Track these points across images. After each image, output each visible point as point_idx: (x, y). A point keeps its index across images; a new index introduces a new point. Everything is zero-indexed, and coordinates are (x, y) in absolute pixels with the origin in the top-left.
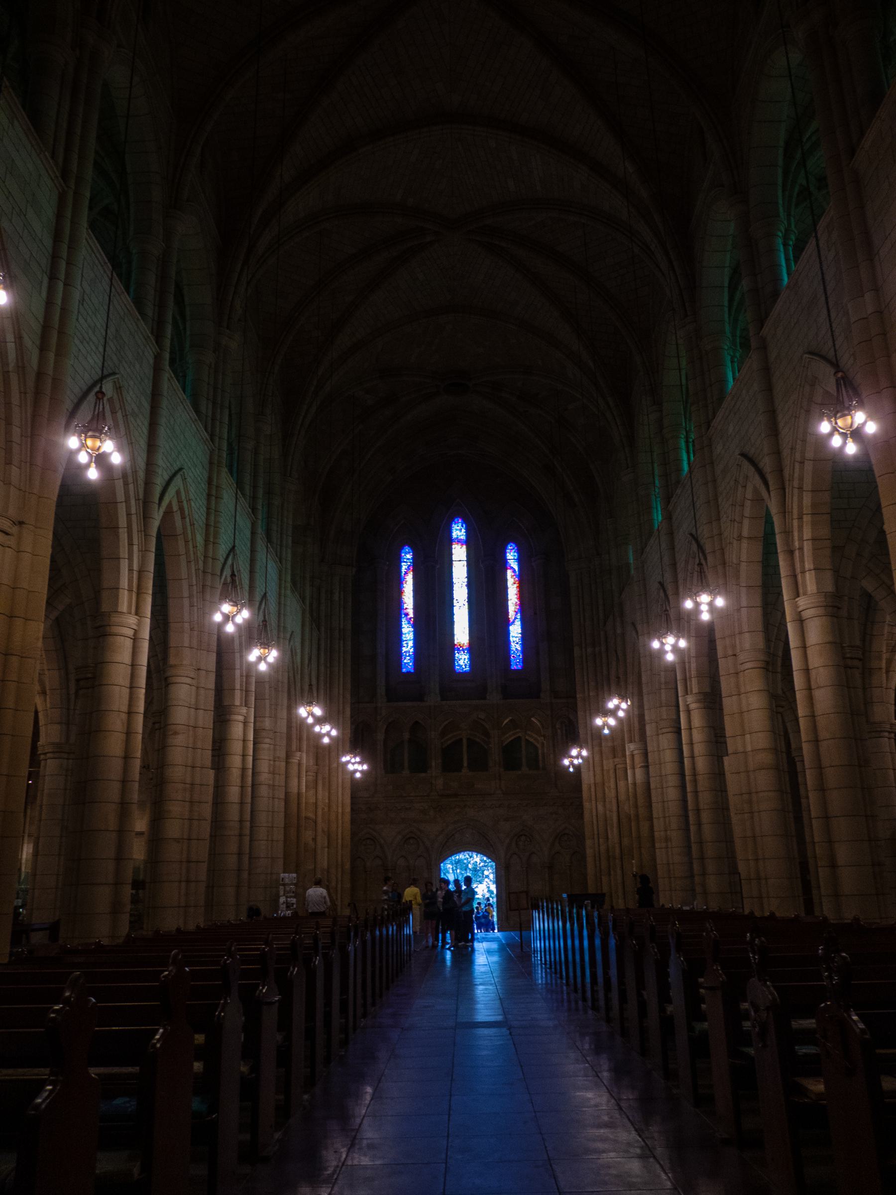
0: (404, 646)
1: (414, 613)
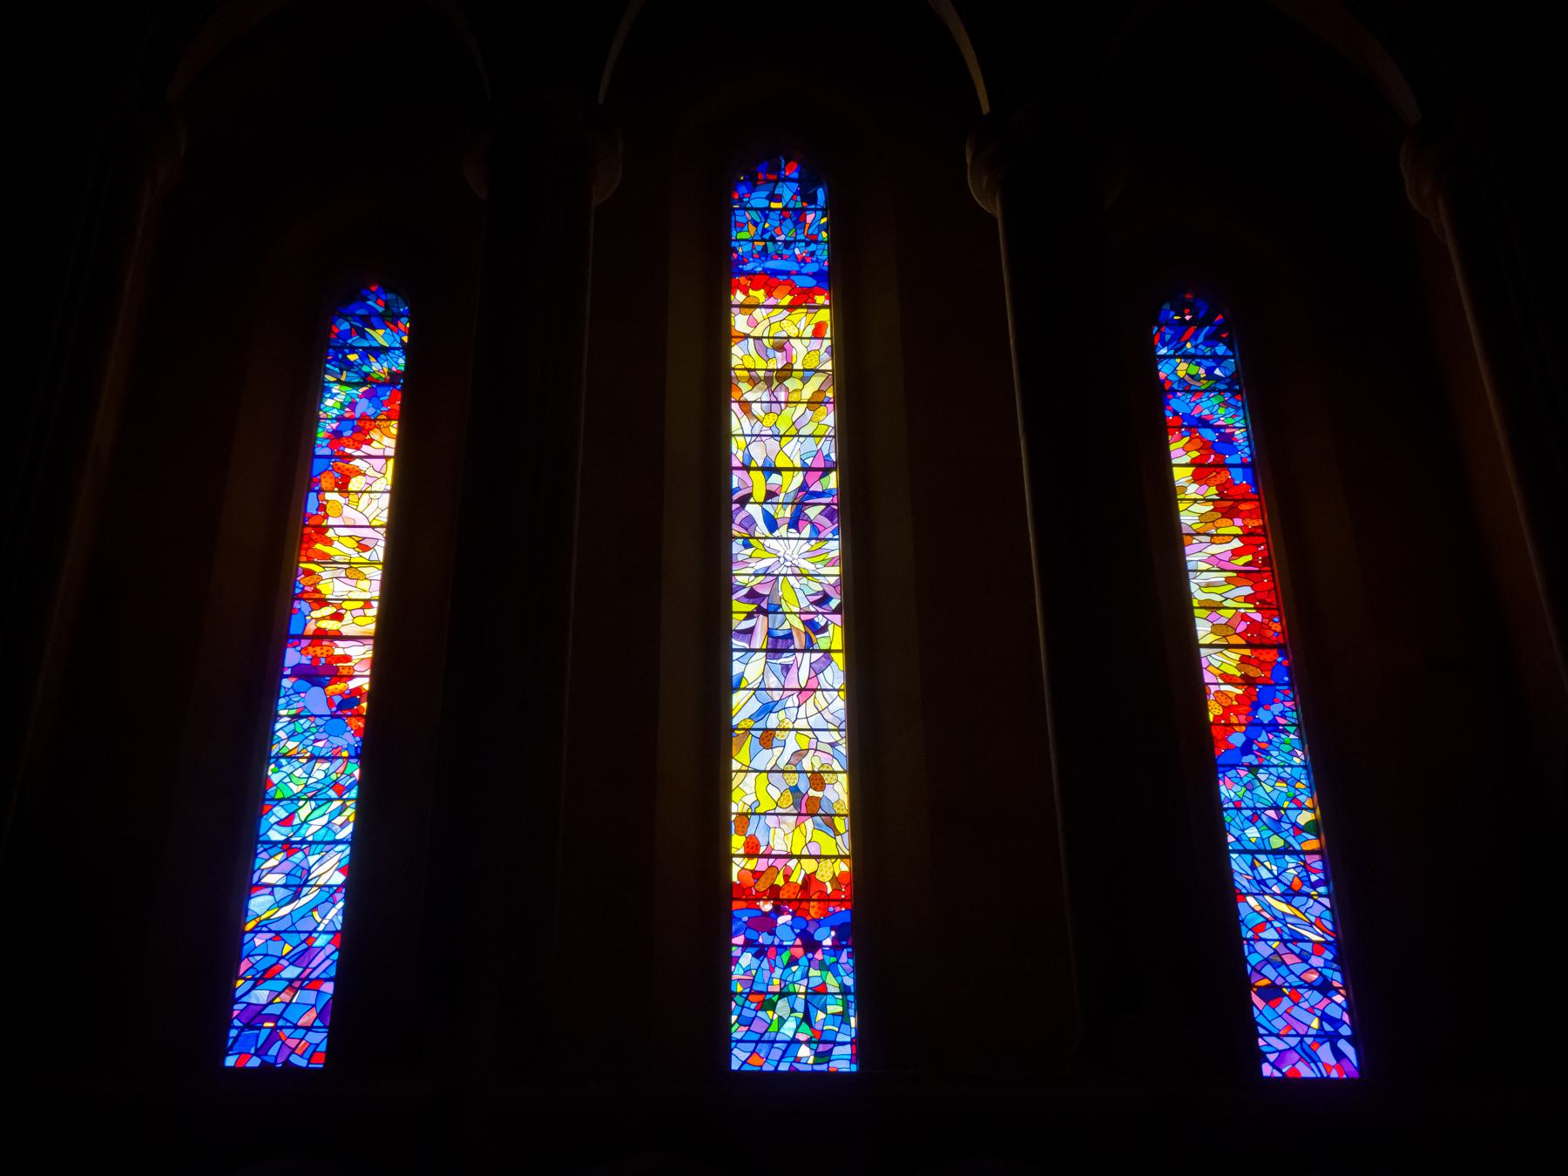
0: (273, 886)
1: (380, 666)
